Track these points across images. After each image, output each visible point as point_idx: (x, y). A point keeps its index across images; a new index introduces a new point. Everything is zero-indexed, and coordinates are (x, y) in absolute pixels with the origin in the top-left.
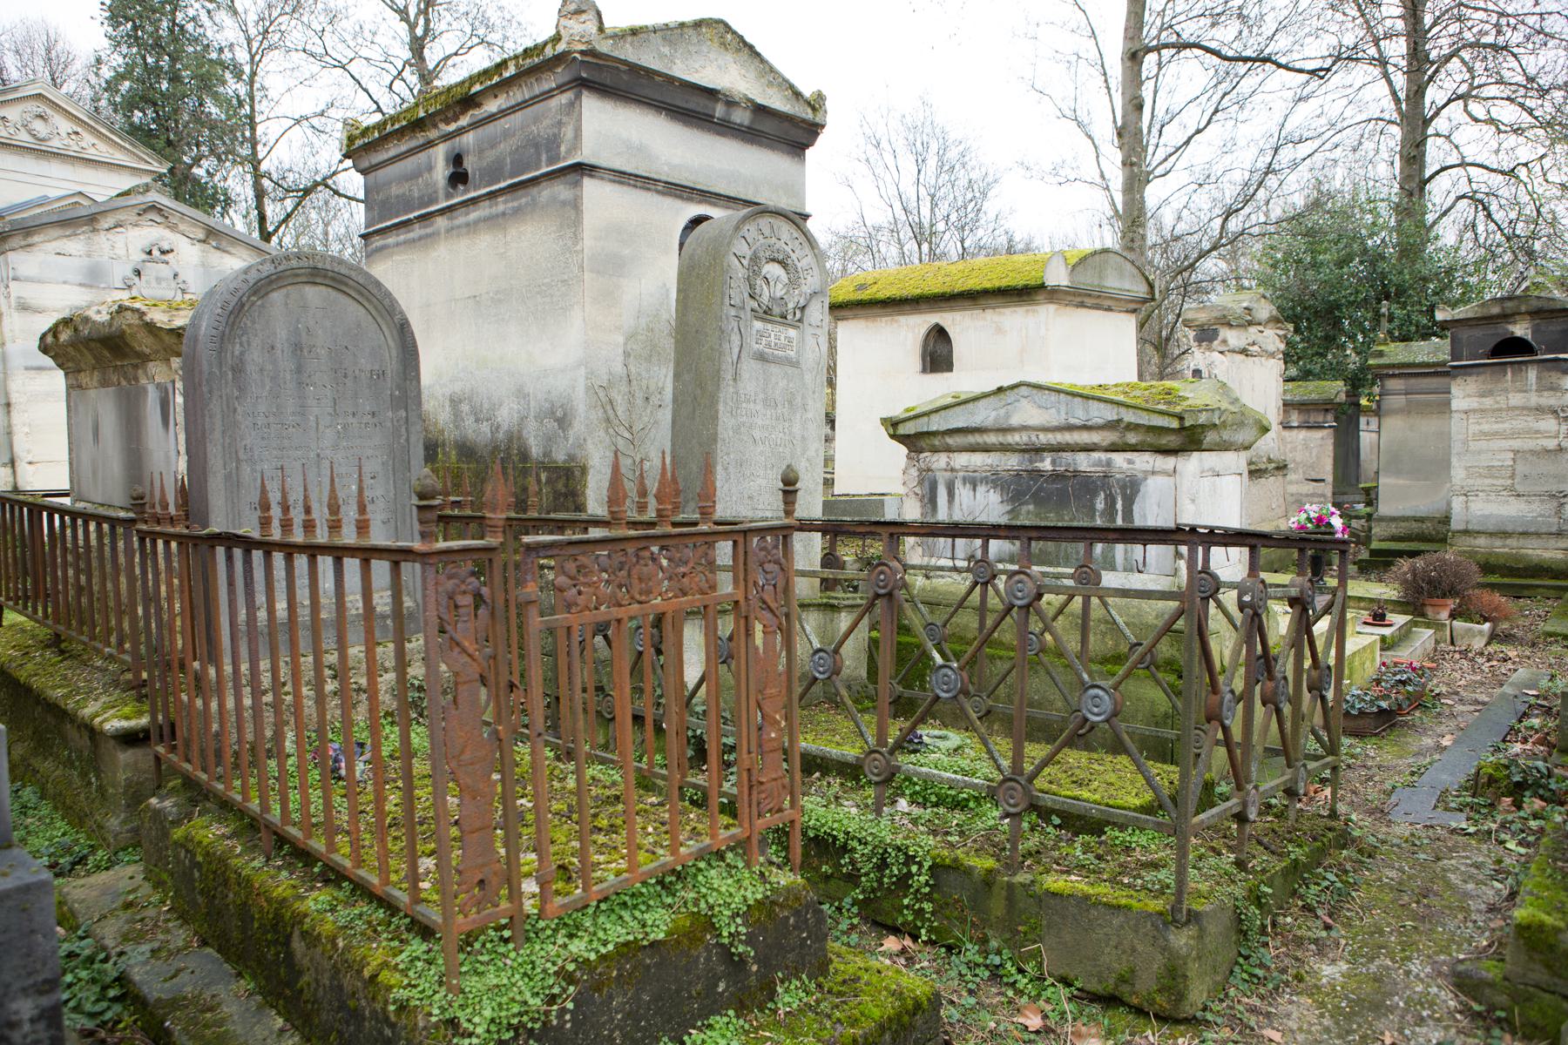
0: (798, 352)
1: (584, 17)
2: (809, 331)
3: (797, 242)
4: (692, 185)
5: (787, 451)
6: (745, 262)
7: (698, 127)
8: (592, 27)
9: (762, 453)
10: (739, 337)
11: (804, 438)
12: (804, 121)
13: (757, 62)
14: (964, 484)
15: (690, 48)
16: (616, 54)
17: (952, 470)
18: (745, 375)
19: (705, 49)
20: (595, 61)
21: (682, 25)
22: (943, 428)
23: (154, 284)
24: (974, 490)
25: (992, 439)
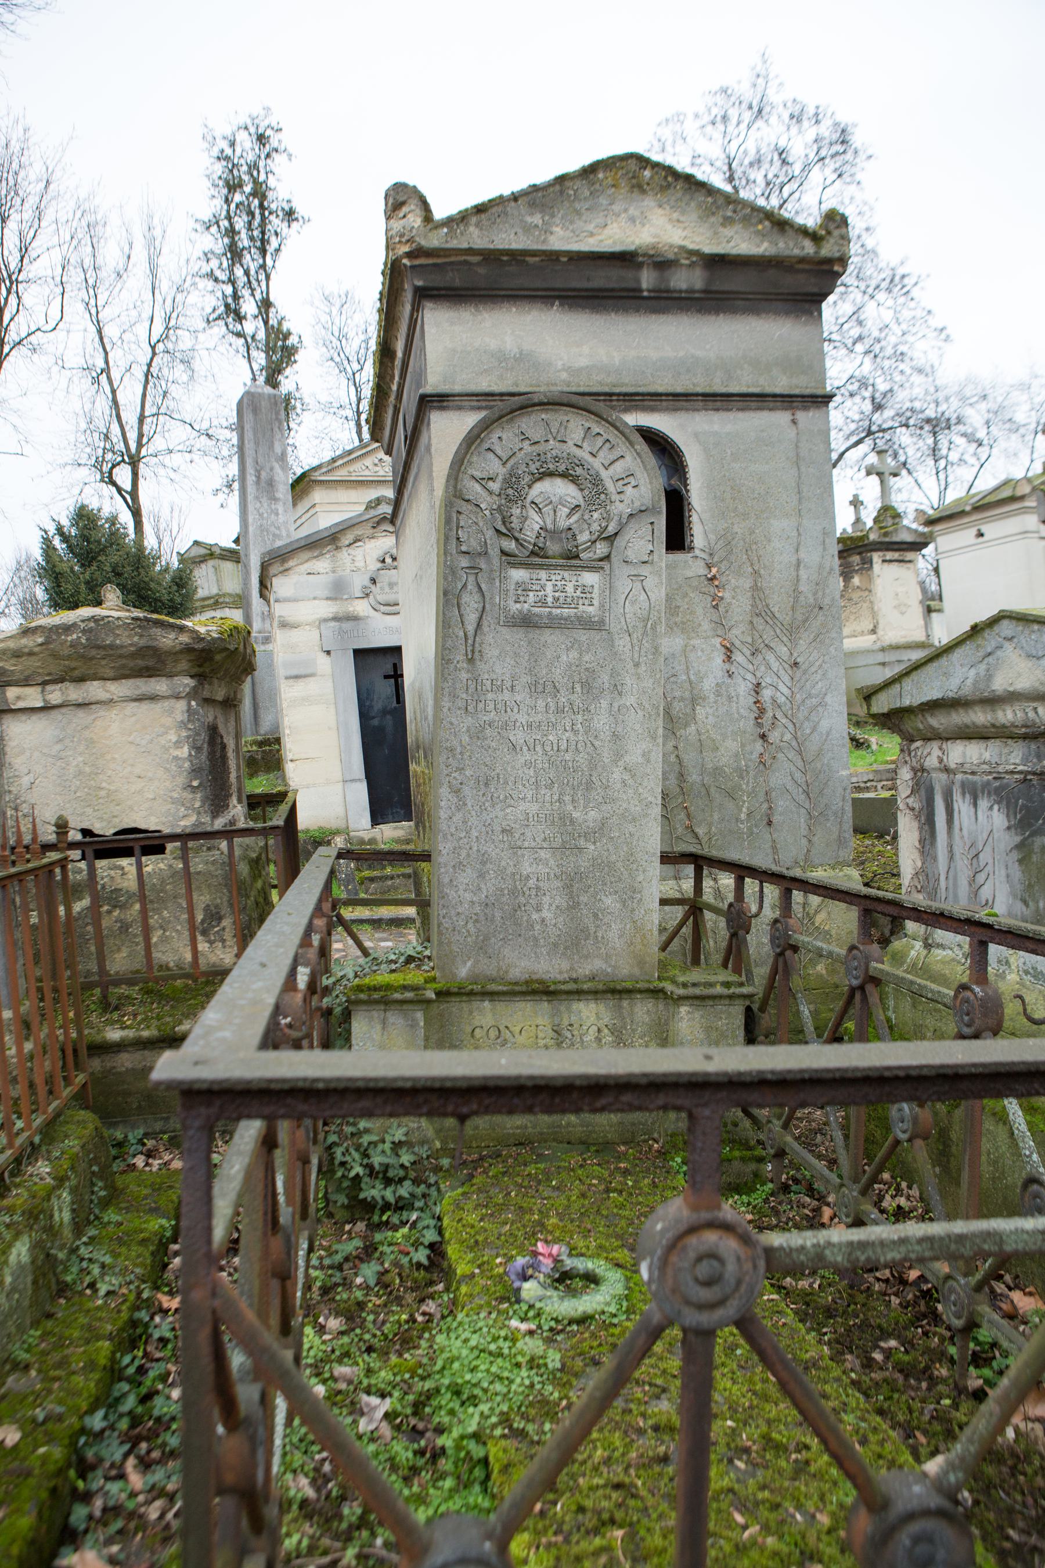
0: (602, 606)
1: (405, 209)
2: (621, 572)
3: (600, 441)
4: (607, 389)
5: (582, 759)
6: (495, 486)
7: (616, 309)
8: (415, 220)
9: (528, 764)
10: (477, 597)
11: (616, 736)
12: (802, 260)
13: (700, 197)
14: (963, 794)
15: (577, 206)
16: (454, 244)
17: (947, 770)
18: (491, 652)
19: (603, 201)
20: (430, 261)
21: (561, 179)
22: (916, 702)
23: (387, 589)
24: (975, 805)
25: (979, 717)
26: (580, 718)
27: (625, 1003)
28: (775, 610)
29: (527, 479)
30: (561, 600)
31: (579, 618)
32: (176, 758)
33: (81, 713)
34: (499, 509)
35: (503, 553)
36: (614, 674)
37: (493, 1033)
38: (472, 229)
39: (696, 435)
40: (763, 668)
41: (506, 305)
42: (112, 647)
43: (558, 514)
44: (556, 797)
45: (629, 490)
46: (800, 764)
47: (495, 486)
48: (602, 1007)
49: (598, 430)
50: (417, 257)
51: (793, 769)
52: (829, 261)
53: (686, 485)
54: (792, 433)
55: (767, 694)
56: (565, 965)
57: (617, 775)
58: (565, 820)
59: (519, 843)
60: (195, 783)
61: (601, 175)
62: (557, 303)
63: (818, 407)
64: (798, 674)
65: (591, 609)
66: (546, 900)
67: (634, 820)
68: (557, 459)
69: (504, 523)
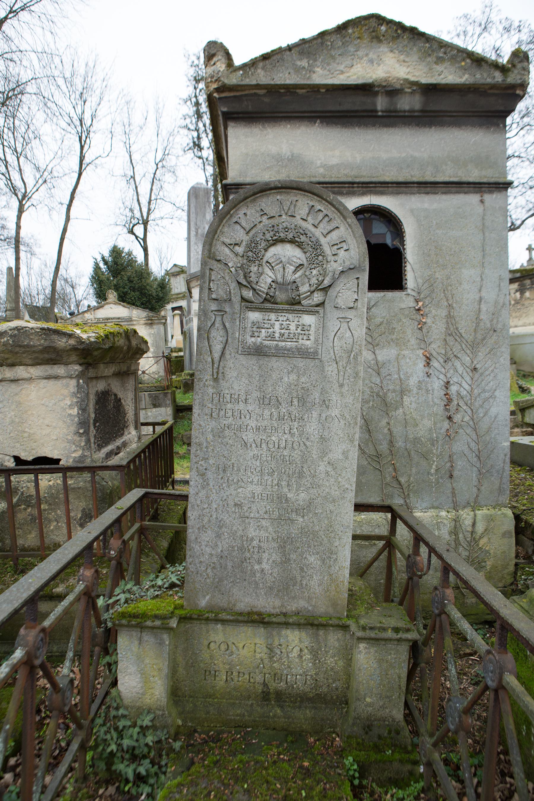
0: (316, 340)
1: (215, 59)
2: (333, 315)
3: (321, 216)
4: (350, 180)
5: (296, 455)
6: (240, 250)
7: (360, 125)
8: (221, 66)
10: (222, 332)
12: (493, 86)
15: (333, 53)
16: (247, 81)
18: (231, 374)
19: (351, 49)
20: (232, 94)
21: (323, 34)
26: (296, 424)
27: (321, 632)
28: (462, 331)
29: (263, 244)
30: (286, 336)
31: (299, 350)
32: (70, 415)
33: (13, 385)
34: (242, 267)
35: (243, 299)
36: (323, 391)
37: (223, 647)
38: (259, 71)
39: (412, 211)
40: (452, 371)
41: (283, 123)
42: (28, 346)
43: (287, 271)
44: (275, 482)
45: (342, 253)
46: (474, 437)
47: (240, 250)
48: (304, 634)
49: (319, 207)
50: (223, 92)
51: (470, 440)
52: (513, 87)
53: (404, 245)
54: (479, 209)
55: (454, 389)
56: (278, 603)
57: (322, 467)
58: (282, 499)
59: (247, 514)
60: (81, 431)
61: (350, 31)
62: (318, 121)
63: (500, 191)
64: (477, 376)
65: (308, 342)
66: (265, 556)
67: (334, 501)
68: (286, 229)
69: (245, 277)
